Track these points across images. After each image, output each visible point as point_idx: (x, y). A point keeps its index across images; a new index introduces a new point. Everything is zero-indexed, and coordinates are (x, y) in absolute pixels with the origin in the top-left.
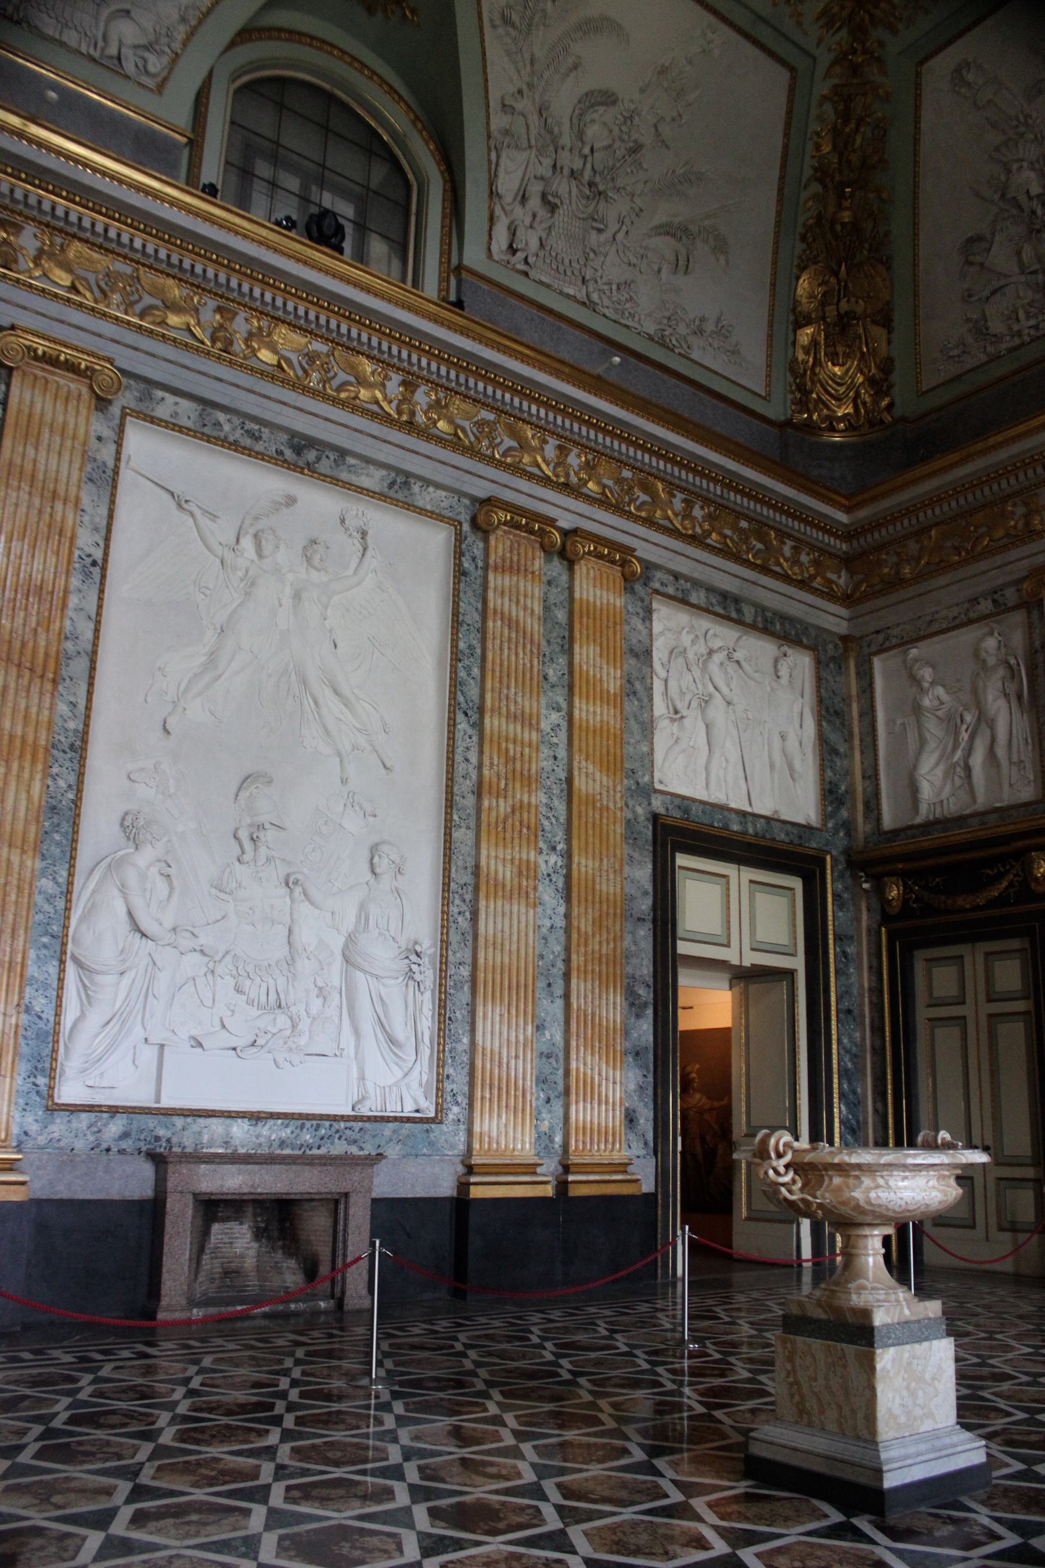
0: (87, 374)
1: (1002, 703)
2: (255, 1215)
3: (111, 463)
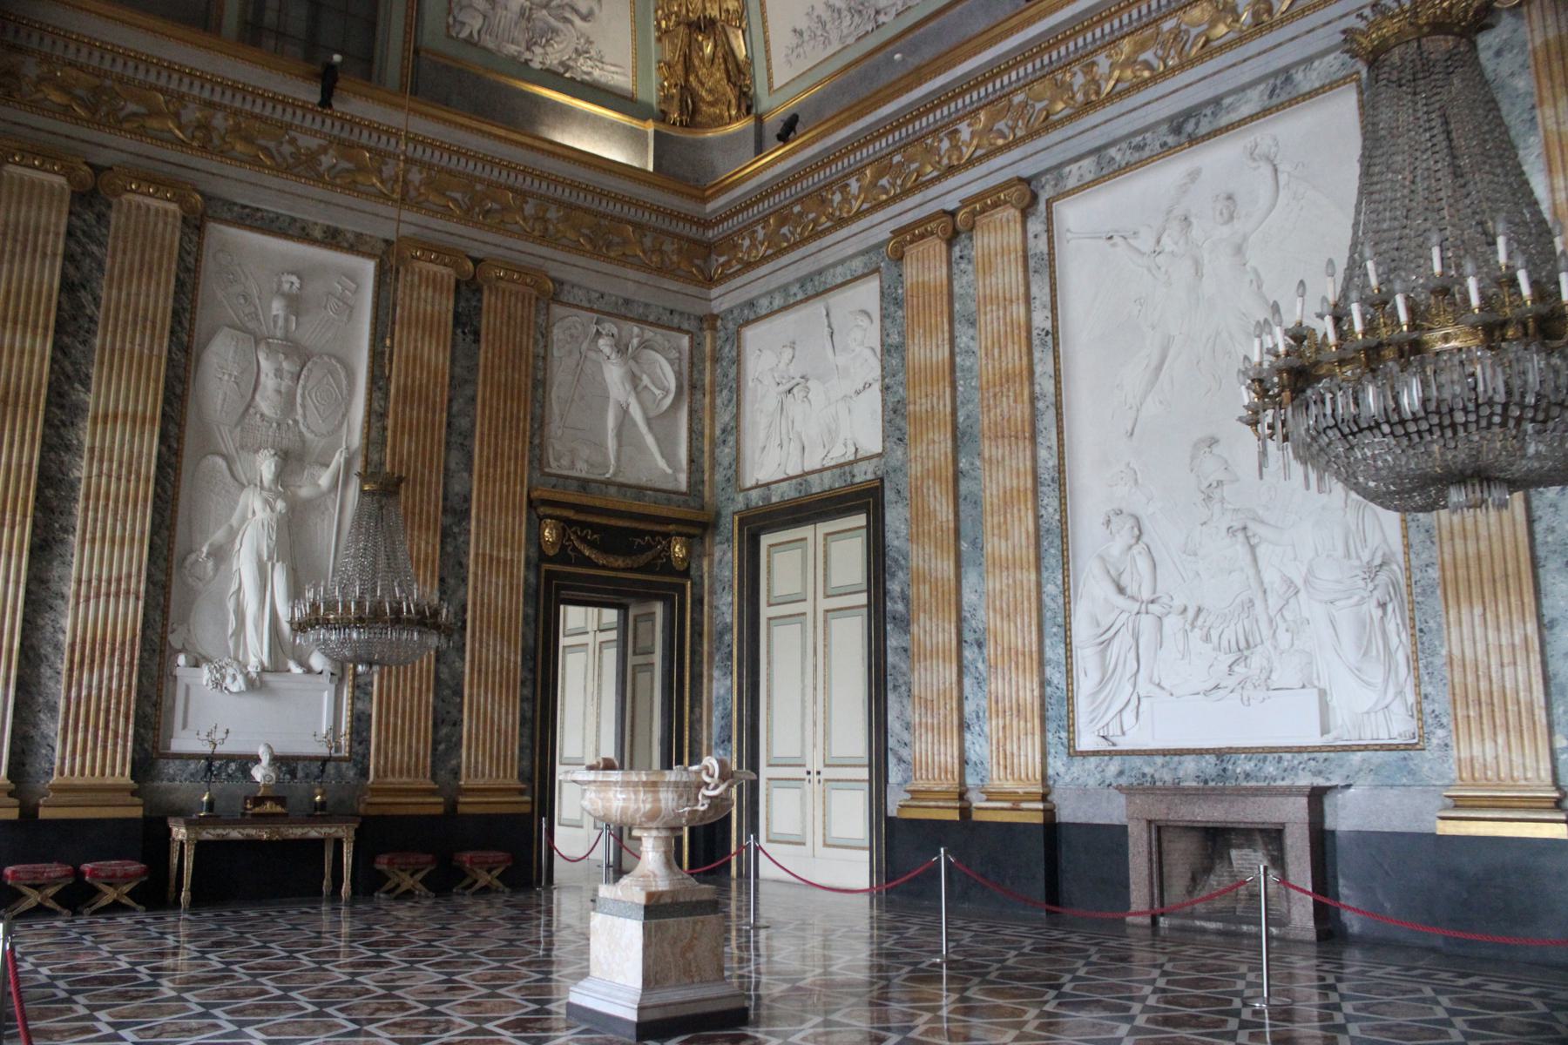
2: (1266, 845)
3: (1046, 250)
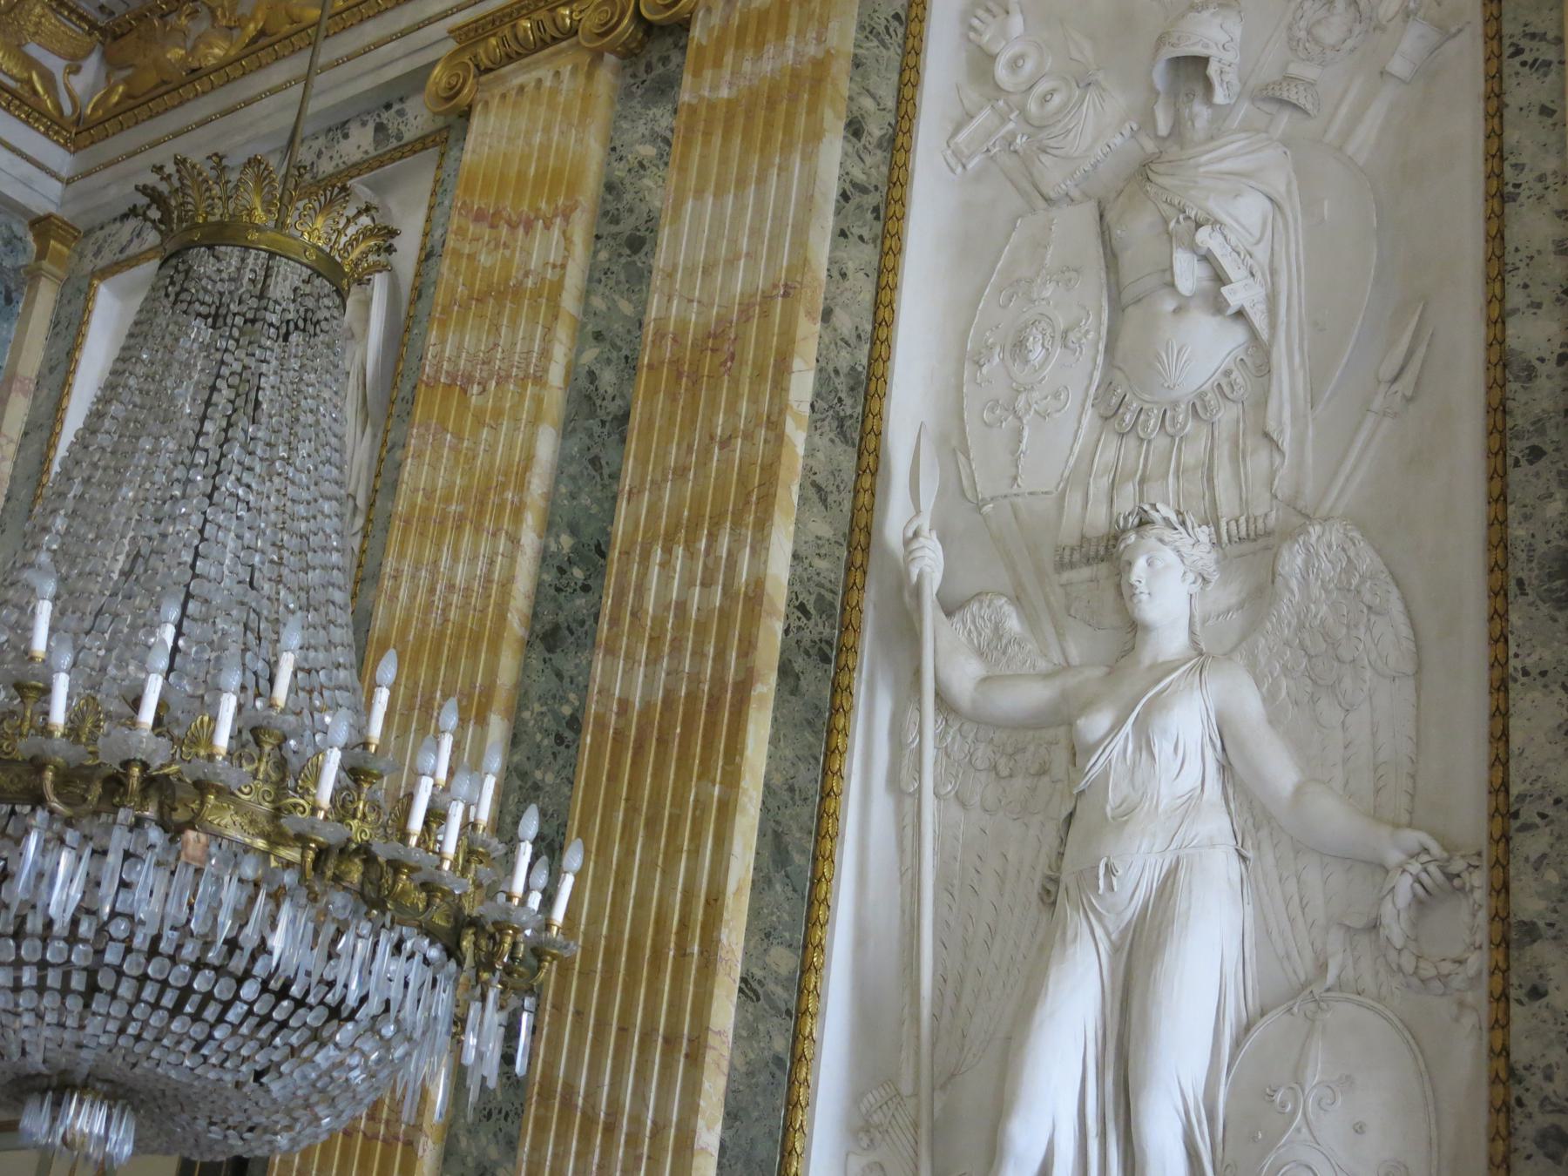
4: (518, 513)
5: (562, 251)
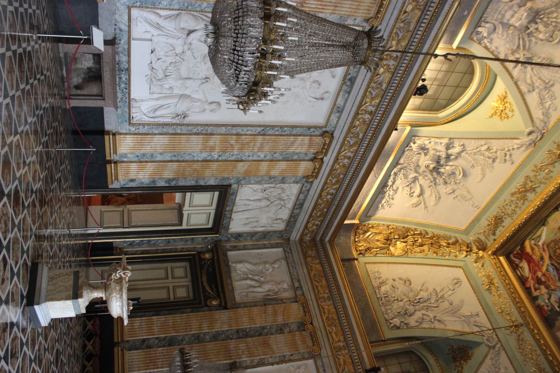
0: (376, 17)
1: (267, 289)
2: (96, 68)
4: (251, 325)
5: (280, 320)
